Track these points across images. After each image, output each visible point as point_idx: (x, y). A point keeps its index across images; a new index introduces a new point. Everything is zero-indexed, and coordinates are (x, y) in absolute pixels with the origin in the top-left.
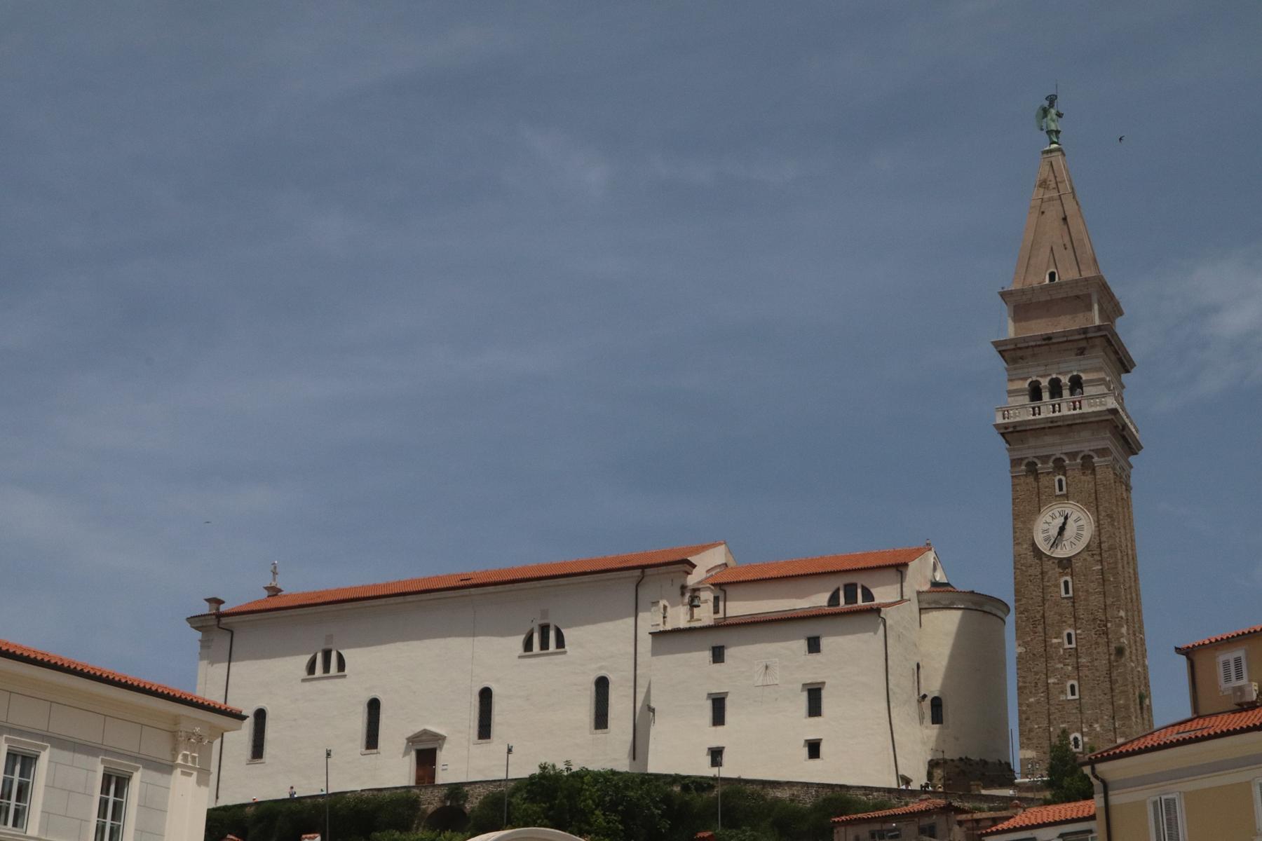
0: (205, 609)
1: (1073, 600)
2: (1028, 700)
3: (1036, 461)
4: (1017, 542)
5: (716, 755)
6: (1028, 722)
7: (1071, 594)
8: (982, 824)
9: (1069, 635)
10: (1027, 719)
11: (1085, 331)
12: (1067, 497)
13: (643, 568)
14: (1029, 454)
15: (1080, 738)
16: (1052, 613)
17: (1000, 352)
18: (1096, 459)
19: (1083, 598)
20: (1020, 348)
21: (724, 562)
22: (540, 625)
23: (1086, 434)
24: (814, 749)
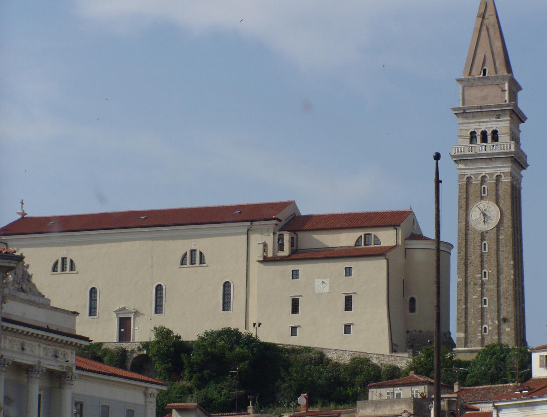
2: (462, 306)
3: (472, 176)
4: (460, 221)
5: (294, 331)
6: (461, 318)
7: (487, 251)
9: (485, 273)
10: (461, 316)
12: (486, 197)
14: (468, 173)
15: (487, 327)
16: (477, 260)
17: (455, 114)
18: (503, 177)
19: (493, 253)
20: (466, 113)
21: (294, 213)
22: (190, 250)
23: (498, 164)
24: (347, 328)
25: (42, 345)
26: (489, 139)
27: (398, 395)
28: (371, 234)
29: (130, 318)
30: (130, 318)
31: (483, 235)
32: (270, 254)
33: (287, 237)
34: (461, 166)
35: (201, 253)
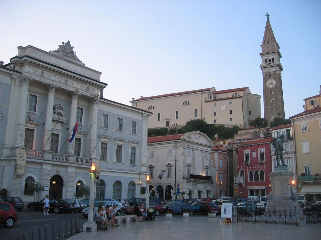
0: (132, 100)
1: (273, 95)
5: (215, 121)
8: (265, 130)
11: (274, 51)
12: (272, 78)
13: (202, 91)
14: (266, 71)
17: (260, 55)
23: (275, 68)
24: (231, 119)
25: (79, 83)
26: (271, 61)
27: (248, 132)
28: (237, 93)
29: (169, 121)
30: (169, 121)
31: (271, 89)
32: (207, 100)
33: (212, 96)
34: (263, 70)
35: (188, 102)
